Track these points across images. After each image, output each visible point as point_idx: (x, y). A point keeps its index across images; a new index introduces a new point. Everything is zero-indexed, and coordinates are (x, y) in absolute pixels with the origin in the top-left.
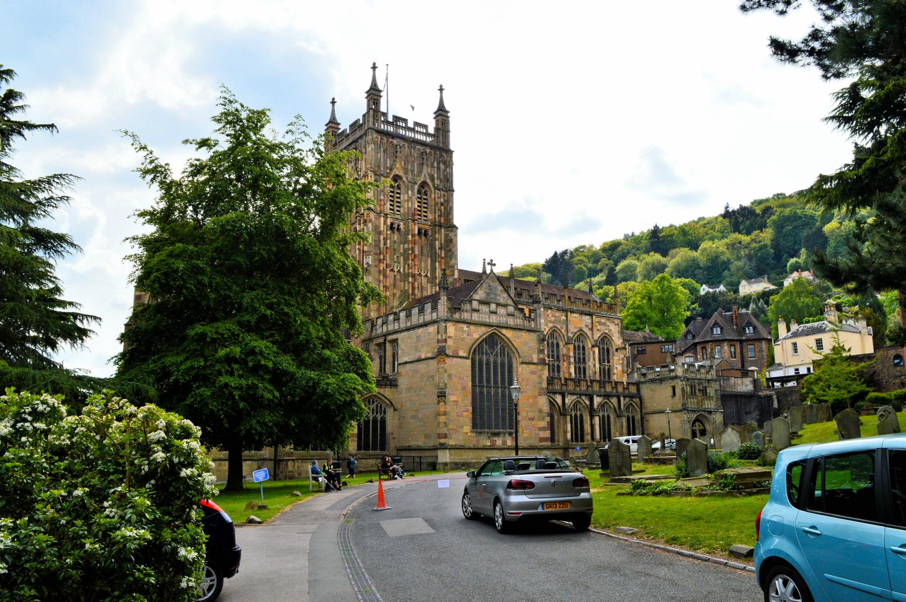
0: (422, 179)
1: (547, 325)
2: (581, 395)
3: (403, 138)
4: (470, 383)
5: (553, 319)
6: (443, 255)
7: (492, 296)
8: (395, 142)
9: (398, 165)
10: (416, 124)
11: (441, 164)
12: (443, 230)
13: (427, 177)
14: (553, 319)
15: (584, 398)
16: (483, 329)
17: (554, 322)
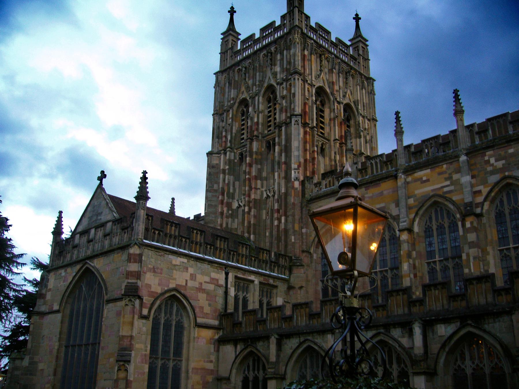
0: (266, 85)
1: (484, 182)
2: (387, 327)
3: (248, 57)
4: (56, 345)
5: (500, 164)
6: (283, 160)
7: (94, 218)
8: (240, 67)
9: (243, 89)
10: (263, 30)
11: (285, 52)
12: (283, 128)
13: (271, 78)
14: (500, 164)
15: (396, 333)
16: (78, 267)
17: (501, 170)
